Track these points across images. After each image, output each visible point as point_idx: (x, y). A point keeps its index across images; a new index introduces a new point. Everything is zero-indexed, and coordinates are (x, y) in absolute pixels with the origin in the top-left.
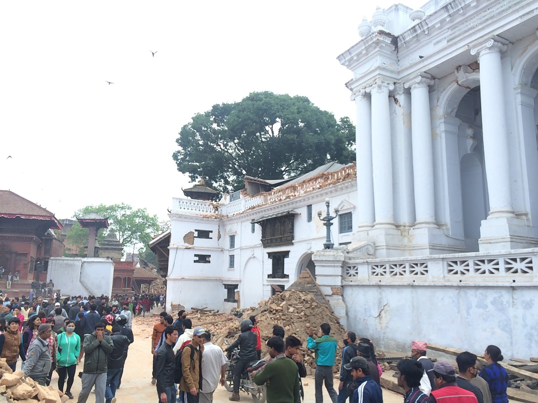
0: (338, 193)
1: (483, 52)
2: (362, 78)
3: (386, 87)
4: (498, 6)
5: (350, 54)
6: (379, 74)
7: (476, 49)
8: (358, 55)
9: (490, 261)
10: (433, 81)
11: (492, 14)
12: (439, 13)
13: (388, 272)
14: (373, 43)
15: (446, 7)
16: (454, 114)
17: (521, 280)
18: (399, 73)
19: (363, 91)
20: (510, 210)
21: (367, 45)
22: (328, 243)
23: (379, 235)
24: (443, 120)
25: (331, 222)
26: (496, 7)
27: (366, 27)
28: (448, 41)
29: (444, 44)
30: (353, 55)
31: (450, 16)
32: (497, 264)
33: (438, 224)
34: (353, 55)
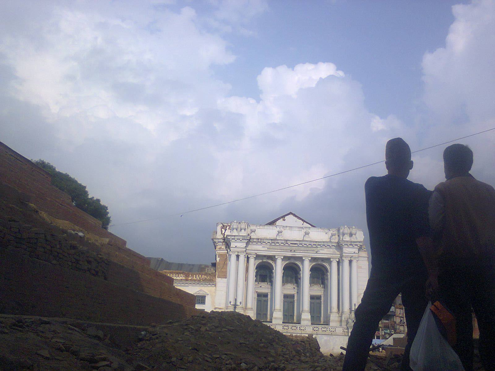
19: (237, 254)
21: (244, 238)
28: (268, 249)
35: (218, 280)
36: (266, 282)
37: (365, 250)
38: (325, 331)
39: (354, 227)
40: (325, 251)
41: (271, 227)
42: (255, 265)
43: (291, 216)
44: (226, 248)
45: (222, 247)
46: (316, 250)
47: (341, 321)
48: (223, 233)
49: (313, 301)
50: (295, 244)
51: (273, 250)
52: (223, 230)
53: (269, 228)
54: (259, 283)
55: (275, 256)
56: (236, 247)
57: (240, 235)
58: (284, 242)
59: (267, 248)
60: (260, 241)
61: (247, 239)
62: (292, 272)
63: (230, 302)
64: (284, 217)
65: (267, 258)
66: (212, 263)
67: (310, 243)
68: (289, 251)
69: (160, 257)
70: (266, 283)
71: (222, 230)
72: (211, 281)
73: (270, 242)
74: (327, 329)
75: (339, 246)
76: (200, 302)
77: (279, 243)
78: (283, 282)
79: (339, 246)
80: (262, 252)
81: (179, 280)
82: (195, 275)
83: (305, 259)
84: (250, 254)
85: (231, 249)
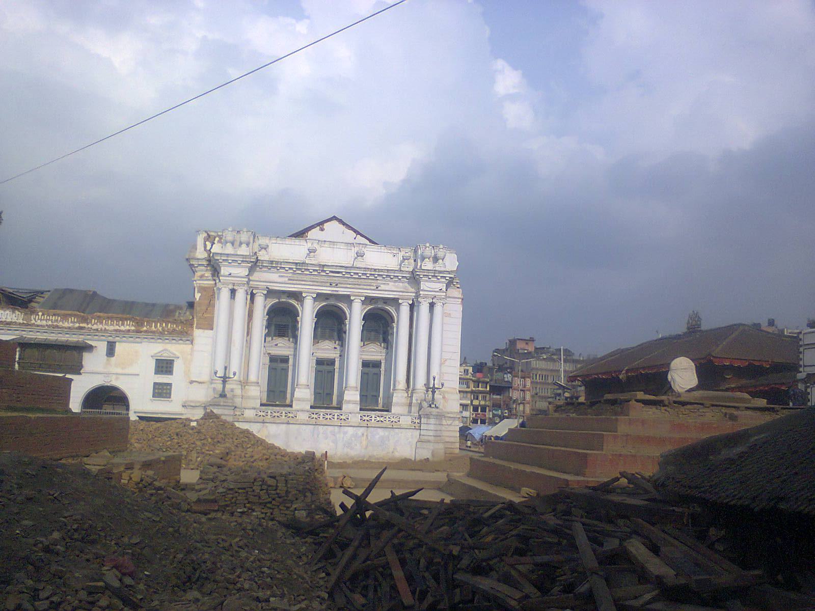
1: (309, 298)
13: (269, 416)
17: (343, 423)
19: (231, 287)
21: (244, 260)
22: (224, 393)
25: (227, 379)
30: (229, 258)
31: (296, 268)
34: (229, 258)
35: (197, 333)
36: (287, 337)
37: (459, 286)
38: (382, 421)
39: (441, 246)
40: (391, 286)
41: (297, 241)
42: (265, 307)
43: (335, 223)
44: (213, 275)
45: (206, 275)
46: (374, 283)
47: (410, 405)
48: (208, 248)
49: (367, 370)
50: (338, 273)
51: (298, 282)
52: (209, 244)
53: (293, 243)
54: (274, 338)
55: (301, 293)
56: (230, 274)
57: (239, 254)
58: (318, 269)
59: (287, 279)
60: (274, 265)
61: (252, 262)
62: (331, 321)
63: (216, 373)
64: (321, 224)
65: (288, 297)
66: (188, 302)
67: (364, 272)
68: (329, 284)
69: (90, 287)
70: (287, 339)
71: (207, 243)
72: (184, 334)
73: (292, 268)
75: (414, 279)
78: (315, 337)
79: (414, 279)
81: (123, 331)
82: (154, 324)
84: (257, 288)
85: (221, 278)
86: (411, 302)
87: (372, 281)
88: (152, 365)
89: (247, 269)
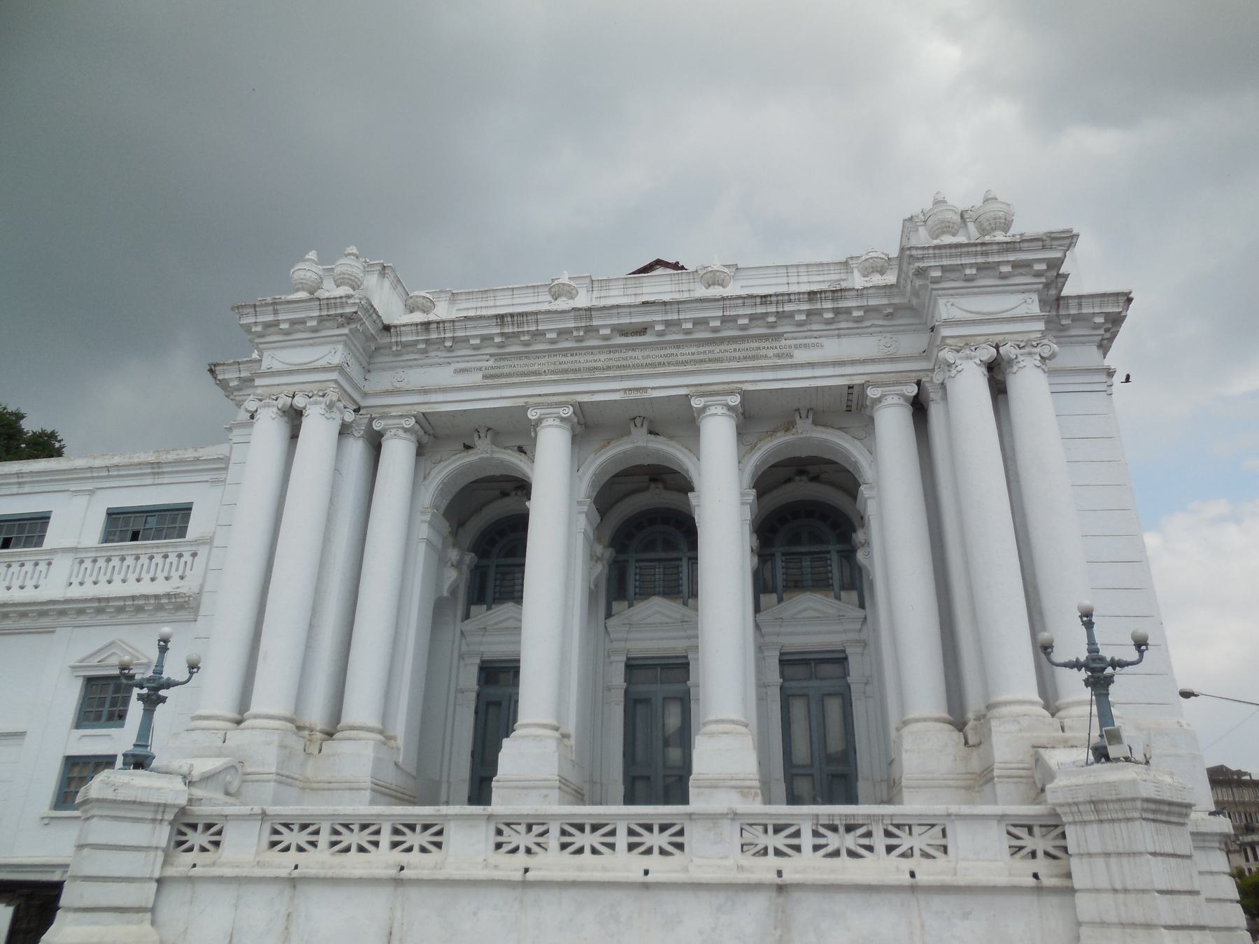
0: (103, 618)
1: (550, 421)
2: (290, 372)
3: (342, 413)
4: (590, 357)
5: (276, 312)
6: (336, 381)
7: (539, 412)
8: (293, 322)
9: (304, 827)
10: (432, 436)
11: (577, 366)
12: (485, 322)
14: (341, 315)
15: (502, 317)
16: (442, 510)
18: (365, 395)
19: (284, 401)
20: (555, 723)
21: (324, 313)
22: (139, 751)
23: (261, 746)
24: (428, 517)
25: (162, 693)
26: (585, 358)
27: (315, 276)
28: (485, 377)
29: (477, 378)
31: (502, 334)
32: (797, 834)
33: (385, 735)
34: (281, 317)
46: (769, 350)
59: (480, 375)
60: (434, 336)
73: (489, 338)
74: (869, 834)
76: (105, 714)
77: (543, 333)
80: (450, 397)
83: (704, 409)
86: (912, 390)
87: (762, 345)
88: (72, 694)
89: (340, 347)
